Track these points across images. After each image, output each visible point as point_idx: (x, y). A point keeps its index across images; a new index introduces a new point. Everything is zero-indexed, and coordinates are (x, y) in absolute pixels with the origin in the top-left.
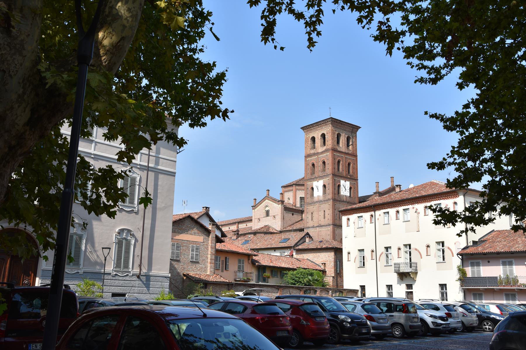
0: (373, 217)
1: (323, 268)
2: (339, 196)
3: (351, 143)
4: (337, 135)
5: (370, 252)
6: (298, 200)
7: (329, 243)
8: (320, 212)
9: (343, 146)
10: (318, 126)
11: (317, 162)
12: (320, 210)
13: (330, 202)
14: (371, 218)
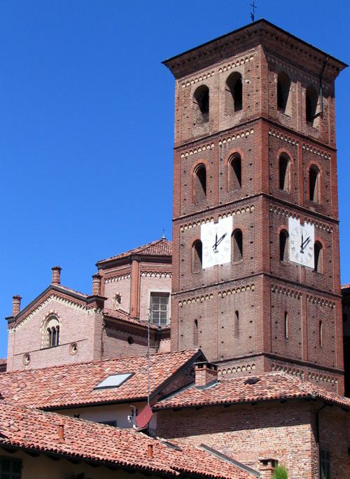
6: (146, 300)
9: (294, 114)
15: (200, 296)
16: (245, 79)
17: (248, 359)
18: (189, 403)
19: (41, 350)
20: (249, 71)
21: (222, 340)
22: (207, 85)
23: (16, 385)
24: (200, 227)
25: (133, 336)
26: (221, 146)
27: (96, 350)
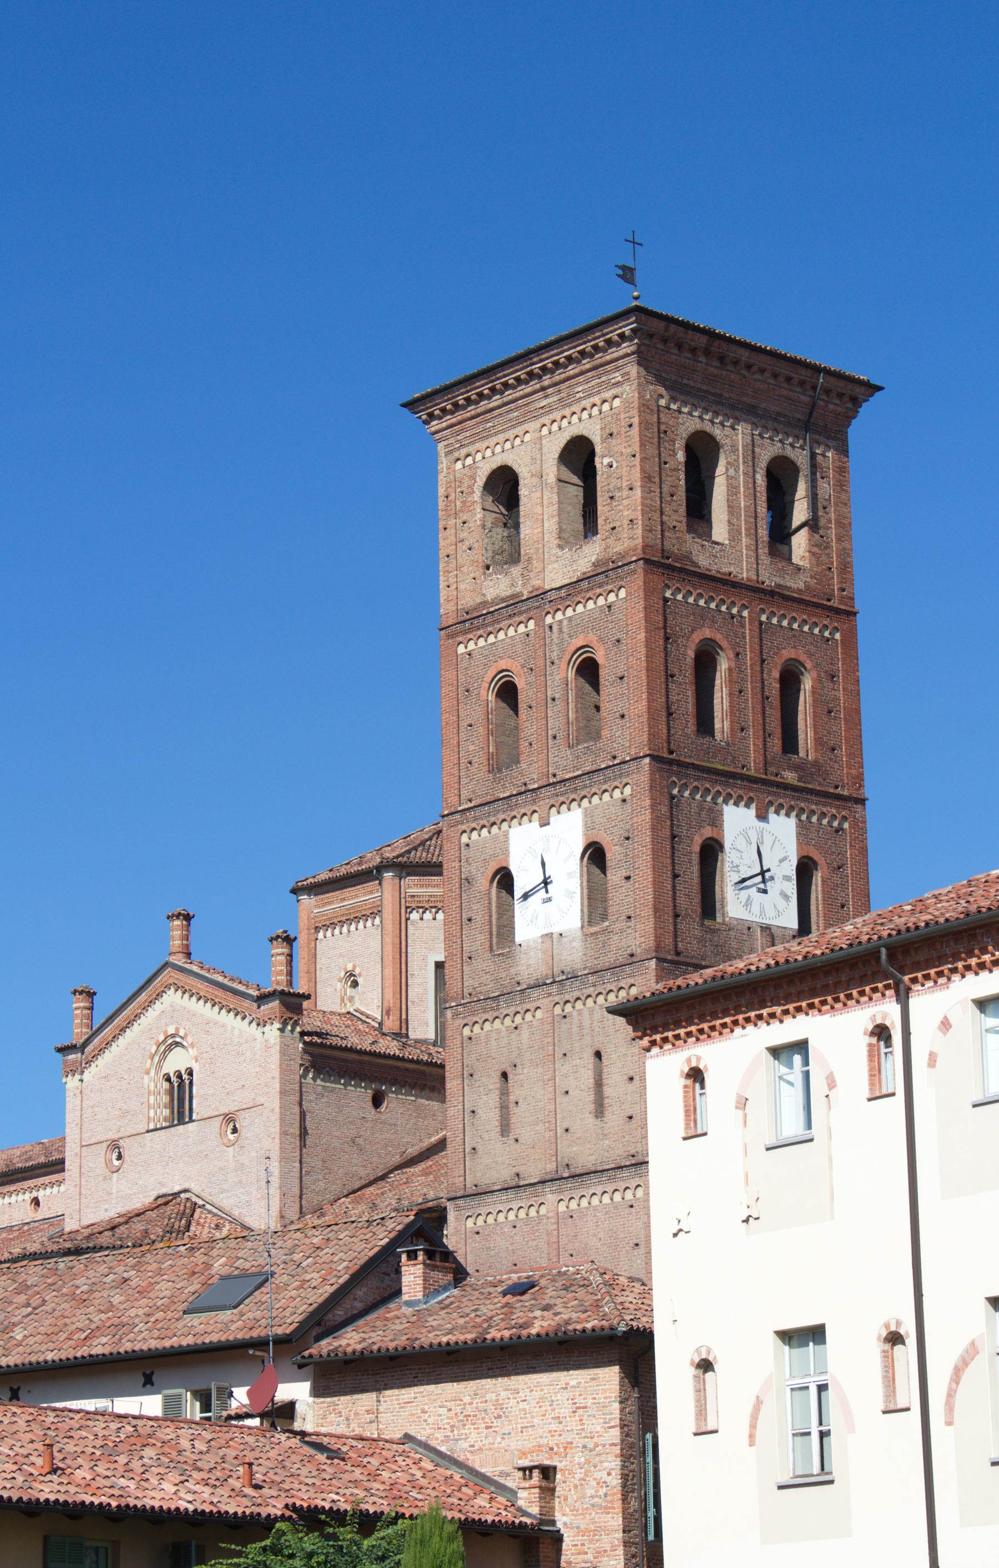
0: (888, 1043)
1: (535, 1510)
2: (714, 931)
3: (800, 513)
4: (689, 449)
5: (876, 1348)
7: (581, 1293)
8: (563, 1068)
9: (734, 534)
10: (534, 385)
11: (539, 671)
12: (565, 1047)
13: (638, 980)
14: (873, 1054)
15: (511, 1010)
16: (603, 457)
17: (626, 1173)
18: (375, 1348)
19: (148, 1131)
20: (611, 435)
21: (565, 1126)
22: (515, 467)
23: (22, 1298)
24: (506, 835)
26: (551, 627)
27: (284, 1133)
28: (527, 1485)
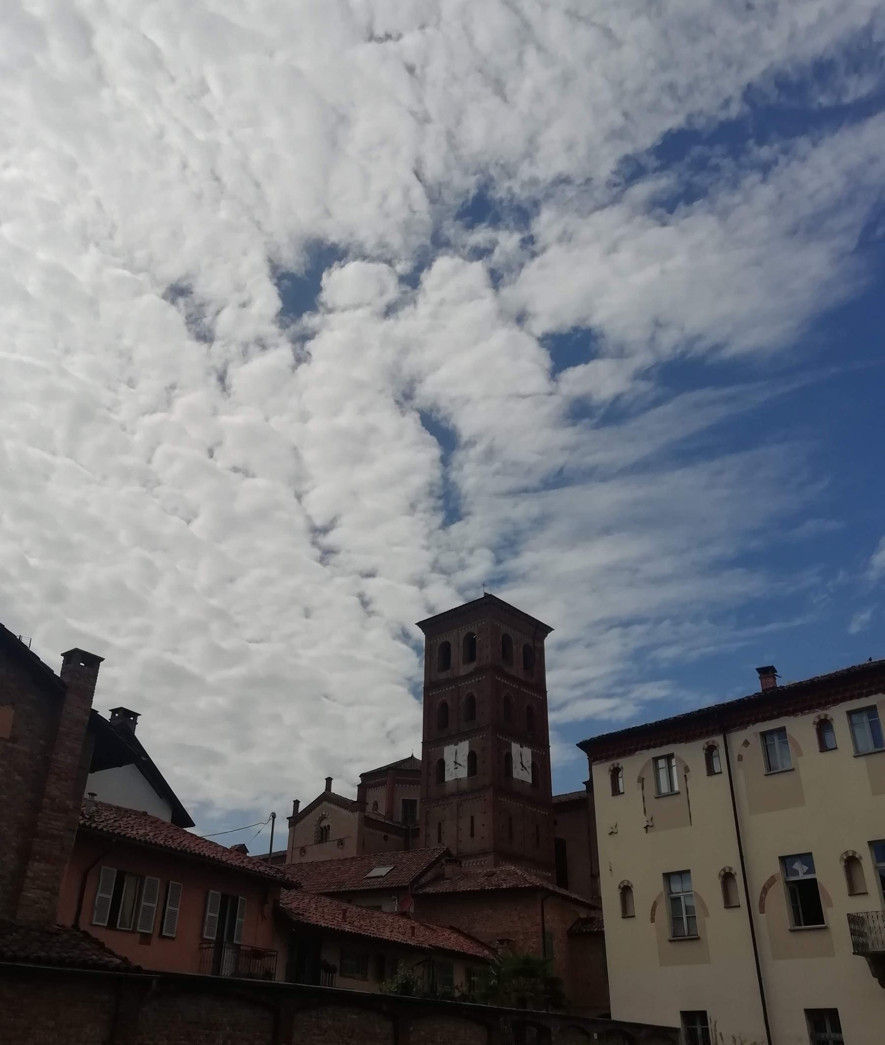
6: (399, 807)
25: (388, 835)
28: (501, 946)
